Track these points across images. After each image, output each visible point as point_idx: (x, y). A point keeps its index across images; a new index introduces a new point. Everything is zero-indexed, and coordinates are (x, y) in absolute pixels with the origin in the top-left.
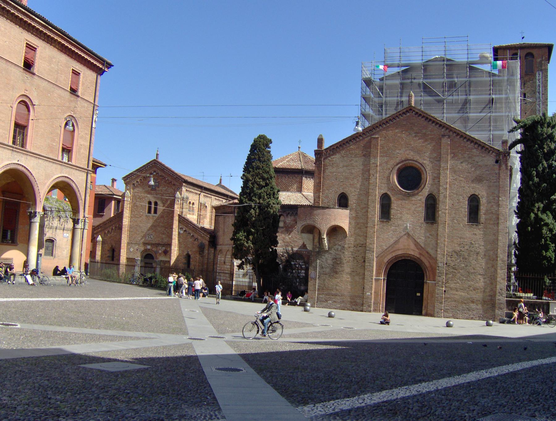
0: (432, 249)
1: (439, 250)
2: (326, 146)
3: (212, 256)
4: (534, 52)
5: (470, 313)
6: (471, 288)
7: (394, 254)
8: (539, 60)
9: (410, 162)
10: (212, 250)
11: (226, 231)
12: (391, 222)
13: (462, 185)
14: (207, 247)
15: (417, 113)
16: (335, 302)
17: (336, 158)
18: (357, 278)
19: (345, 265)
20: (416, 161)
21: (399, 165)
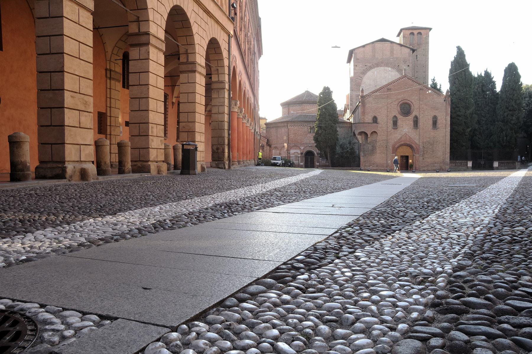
0: (417, 140)
1: (420, 141)
2: (365, 94)
3: (268, 151)
4: (422, 31)
5: (434, 168)
6: (435, 157)
7: (400, 143)
8: (425, 36)
9: (406, 101)
10: (268, 147)
11: (279, 136)
12: (398, 129)
13: (430, 111)
14: (265, 146)
15: (408, 78)
16: (373, 166)
17: (370, 99)
18: (383, 155)
19: (378, 149)
20: (409, 100)
21: (401, 103)
